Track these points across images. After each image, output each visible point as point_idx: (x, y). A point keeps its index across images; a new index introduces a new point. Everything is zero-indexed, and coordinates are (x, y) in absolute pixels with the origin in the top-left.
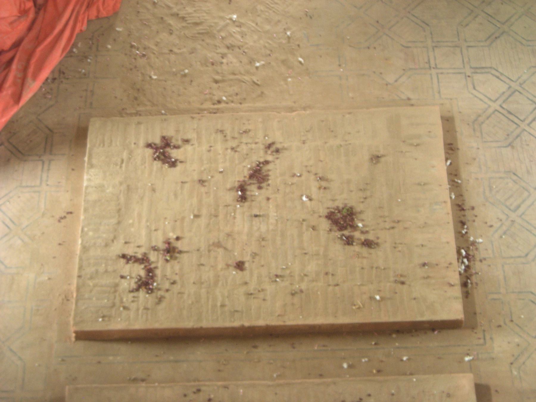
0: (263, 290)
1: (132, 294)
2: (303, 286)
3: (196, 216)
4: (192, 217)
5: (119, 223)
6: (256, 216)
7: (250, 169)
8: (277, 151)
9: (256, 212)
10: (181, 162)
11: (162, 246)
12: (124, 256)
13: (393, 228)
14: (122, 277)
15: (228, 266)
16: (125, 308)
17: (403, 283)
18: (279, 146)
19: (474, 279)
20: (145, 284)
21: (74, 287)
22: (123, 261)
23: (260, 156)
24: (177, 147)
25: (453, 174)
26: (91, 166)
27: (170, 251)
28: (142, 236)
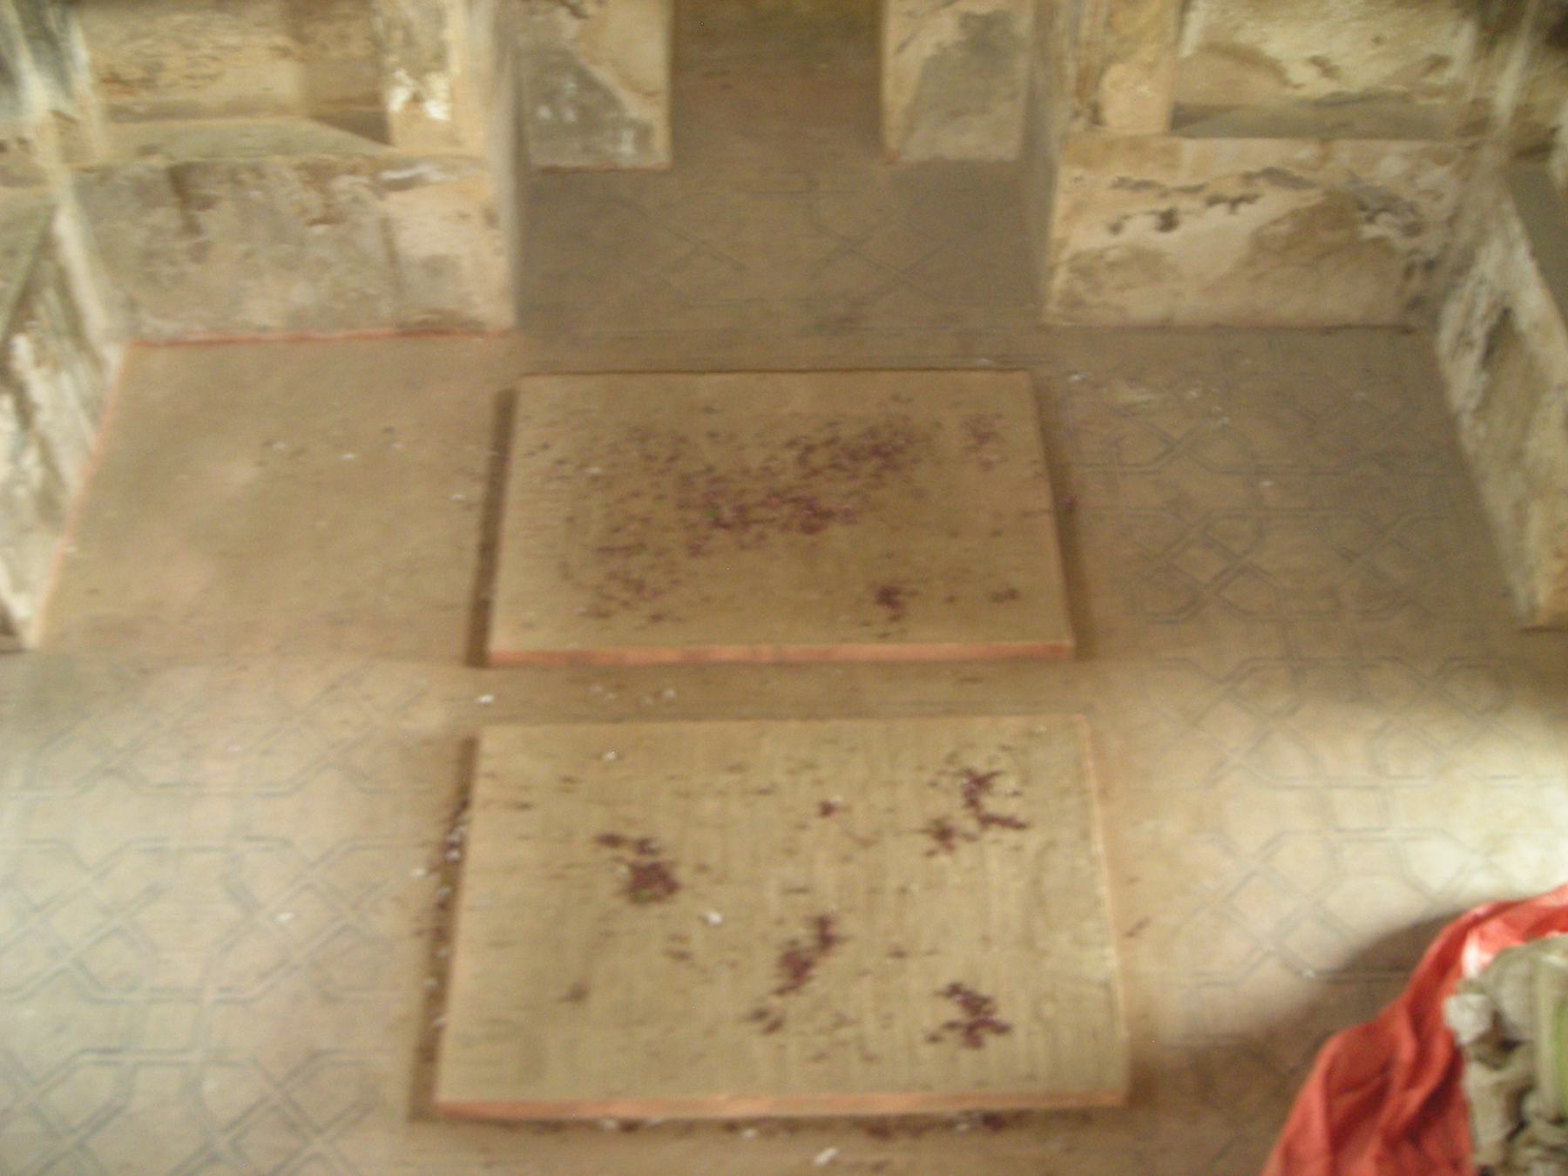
0: (792, 772)
1: (995, 768)
2: (724, 780)
3: (903, 891)
4: (915, 888)
5: (1036, 882)
6: (801, 890)
7: (811, 978)
8: (760, 1015)
9: (802, 899)
10: (938, 994)
11: (956, 841)
12: (1020, 826)
13: (569, 866)
14: (1016, 794)
15: (848, 809)
16: (1005, 748)
17: (568, 780)
18: (759, 1026)
19: (446, 813)
20: (979, 784)
21: (1097, 811)
22: (1022, 818)
23: (795, 1005)
24: (952, 1026)
25: (436, 998)
26: (1106, 986)
27: (943, 834)
28: (994, 862)
